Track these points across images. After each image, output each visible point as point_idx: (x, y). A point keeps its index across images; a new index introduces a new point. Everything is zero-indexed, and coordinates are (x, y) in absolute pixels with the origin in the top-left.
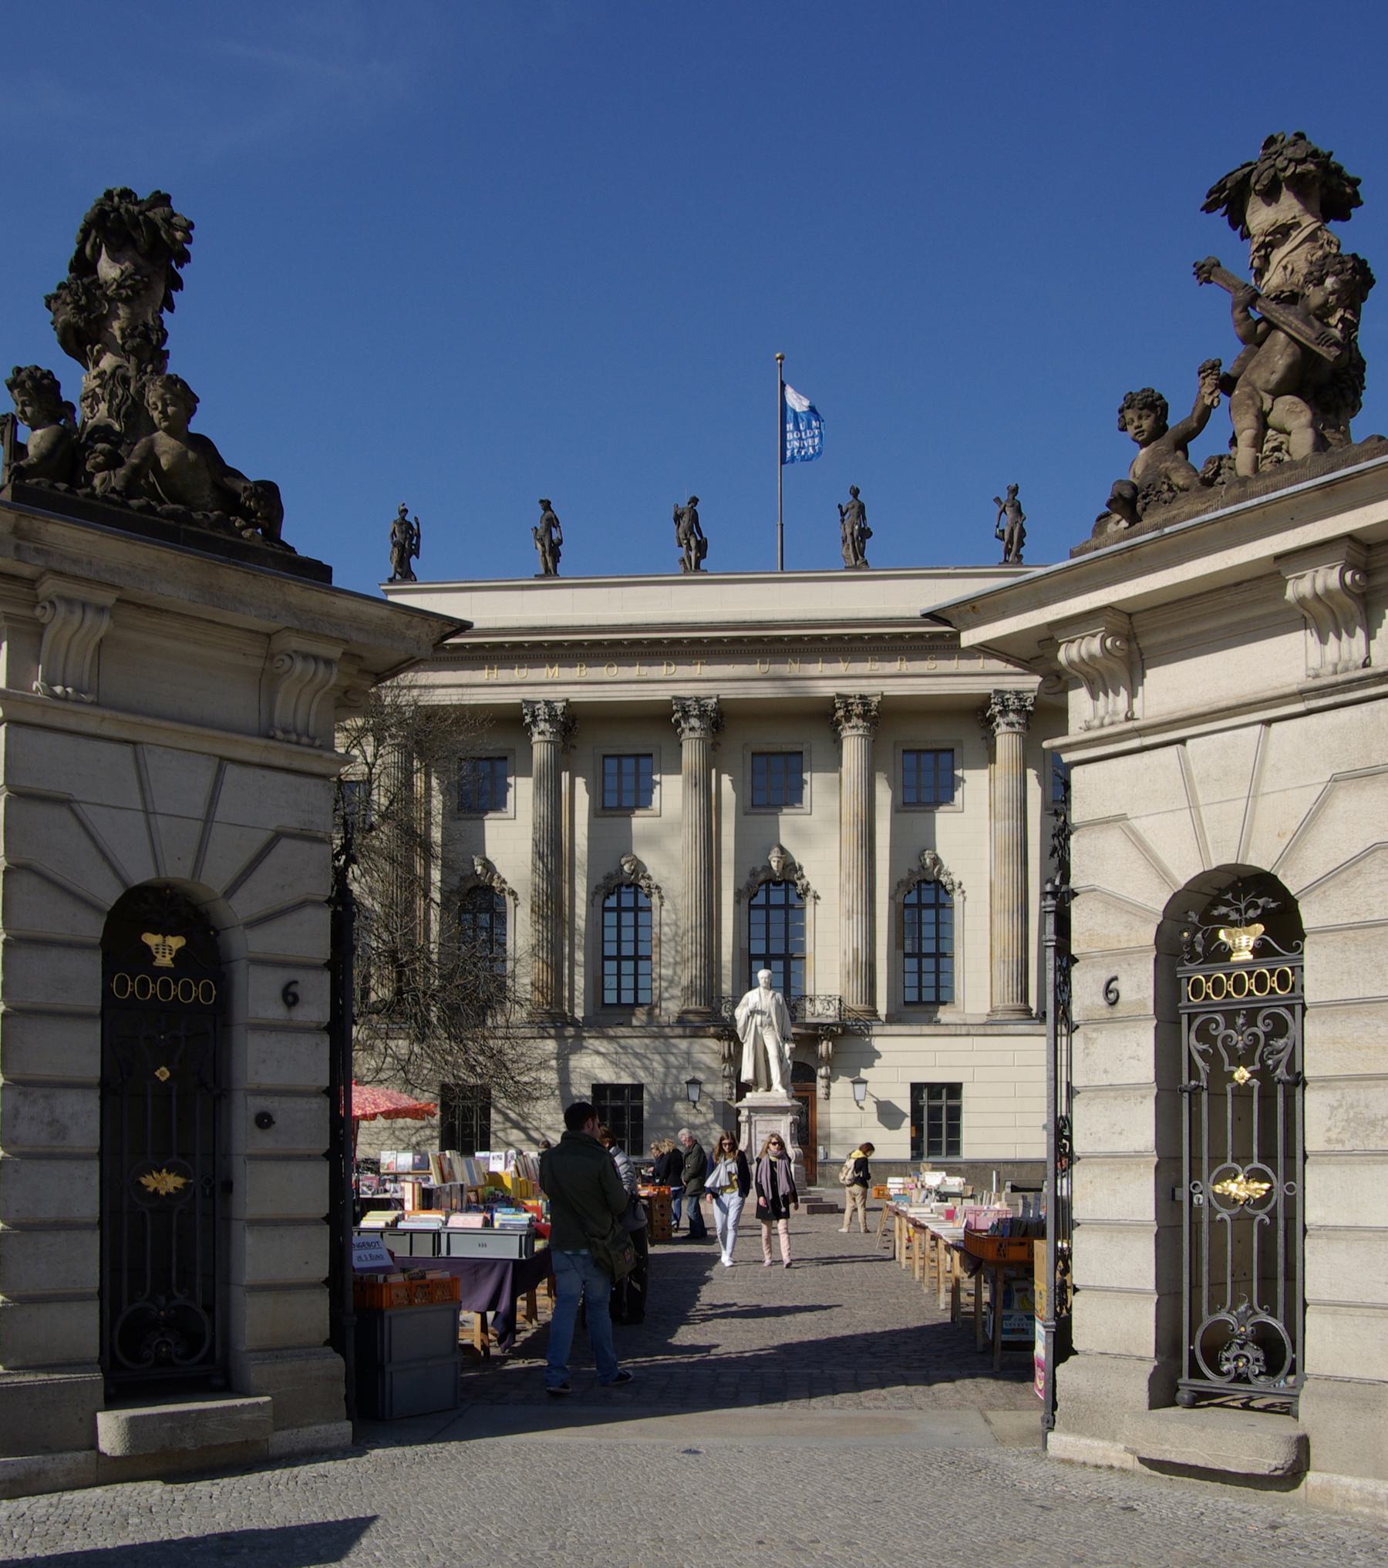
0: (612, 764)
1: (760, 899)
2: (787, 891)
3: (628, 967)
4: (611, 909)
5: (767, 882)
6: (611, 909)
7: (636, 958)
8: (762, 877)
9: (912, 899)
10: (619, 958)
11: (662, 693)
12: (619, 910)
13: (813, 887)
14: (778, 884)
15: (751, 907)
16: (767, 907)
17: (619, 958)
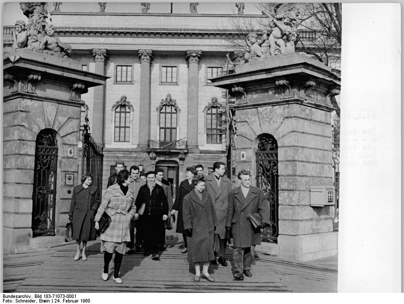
0: (119, 68)
1: (163, 110)
2: (172, 108)
3: (122, 130)
4: (118, 112)
5: (165, 105)
6: (118, 112)
7: (125, 127)
8: (165, 103)
9: (209, 112)
10: (120, 127)
11: (135, 48)
12: (120, 112)
13: (179, 107)
14: (169, 106)
15: (160, 113)
16: (166, 113)
17: (120, 127)
